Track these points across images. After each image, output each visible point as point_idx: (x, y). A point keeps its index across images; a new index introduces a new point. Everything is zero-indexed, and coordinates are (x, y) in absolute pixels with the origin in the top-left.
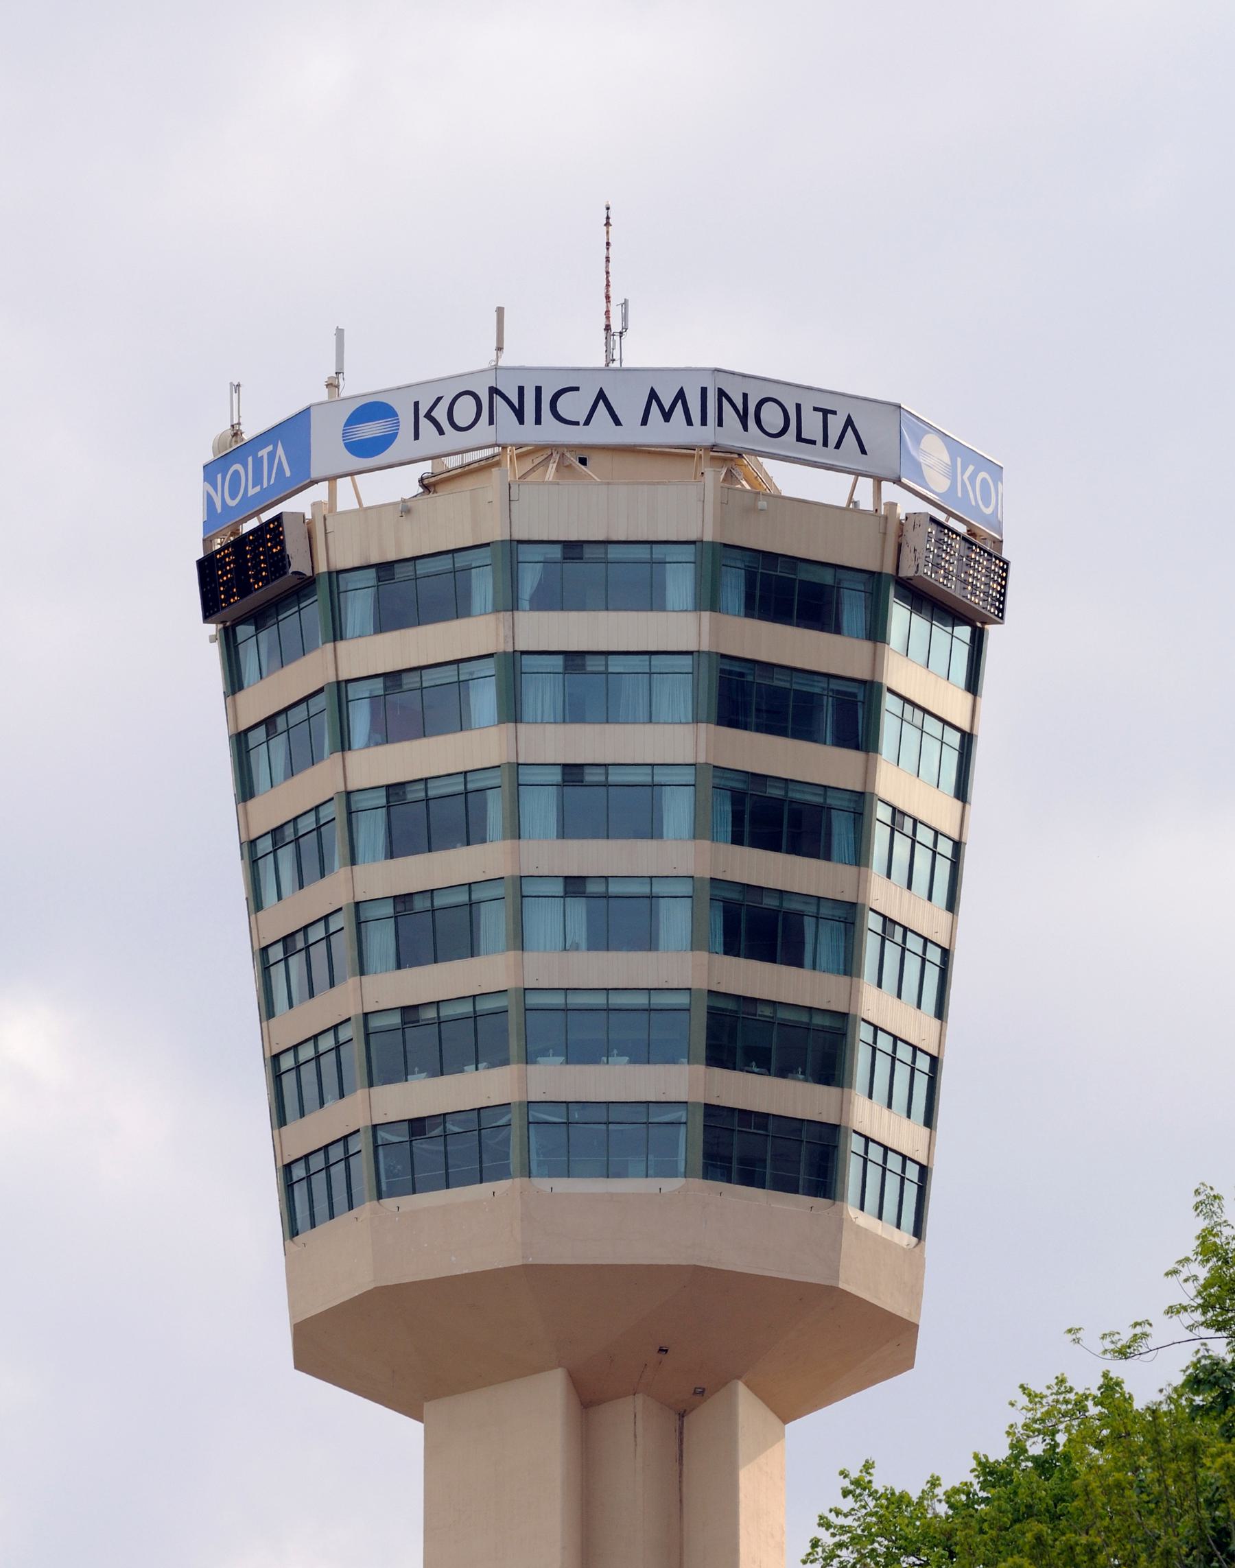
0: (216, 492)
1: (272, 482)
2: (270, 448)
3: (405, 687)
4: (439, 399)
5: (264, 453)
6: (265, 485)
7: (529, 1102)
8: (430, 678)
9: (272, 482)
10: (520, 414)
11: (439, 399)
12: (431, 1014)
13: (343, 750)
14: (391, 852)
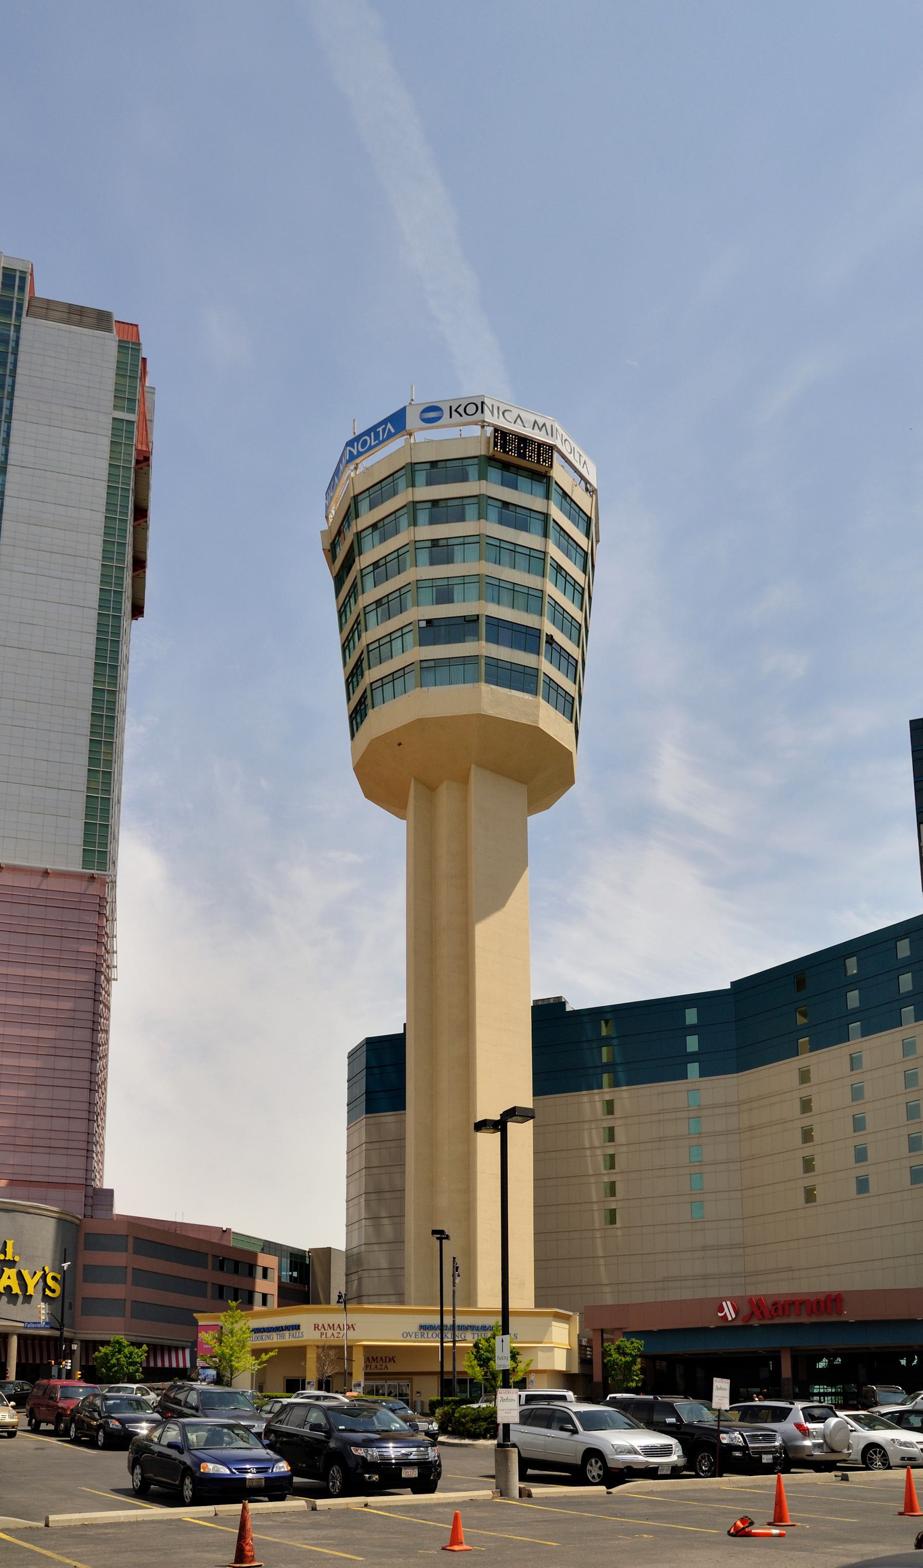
0: (846, 1415)
1: (385, 437)
2: (384, 426)
3: (440, 506)
4: (460, 405)
5: (380, 429)
6: (381, 439)
7: (417, 581)
8: (450, 503)
9: (385, 437)
10: (492, 413)
11: (460, 405)
12: (383, 562)
13: (414, 526)
14: (432, 563)
